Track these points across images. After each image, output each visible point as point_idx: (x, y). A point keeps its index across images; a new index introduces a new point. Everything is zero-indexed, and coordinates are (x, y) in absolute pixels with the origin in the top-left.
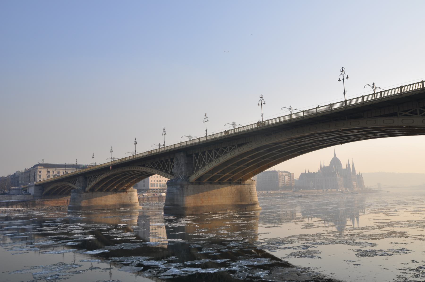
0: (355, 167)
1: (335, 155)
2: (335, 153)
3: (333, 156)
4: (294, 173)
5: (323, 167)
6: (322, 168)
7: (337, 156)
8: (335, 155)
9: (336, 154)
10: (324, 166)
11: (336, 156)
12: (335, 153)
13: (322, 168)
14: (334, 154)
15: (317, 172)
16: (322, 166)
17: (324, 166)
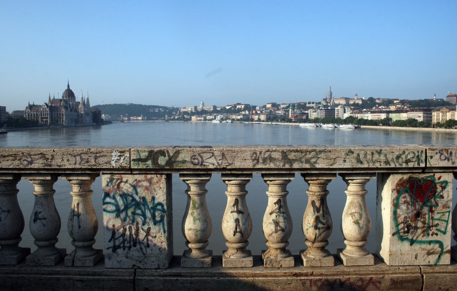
0: (90, 101)
1: (68, 86)
2: (68, 85)
3: (66, 88)
4: (5, 107)
5: (52, 99)
6: (51, 100)
7: (71, 88)
8: (68, 86)
9: (69, 85)
10: (54, 99)
11: (70, 88)
12: (68, 85)
13: (51, 100)
14: (67, 85)
15: (42, 105)
16: (52, 98)
17: (54, 99)
